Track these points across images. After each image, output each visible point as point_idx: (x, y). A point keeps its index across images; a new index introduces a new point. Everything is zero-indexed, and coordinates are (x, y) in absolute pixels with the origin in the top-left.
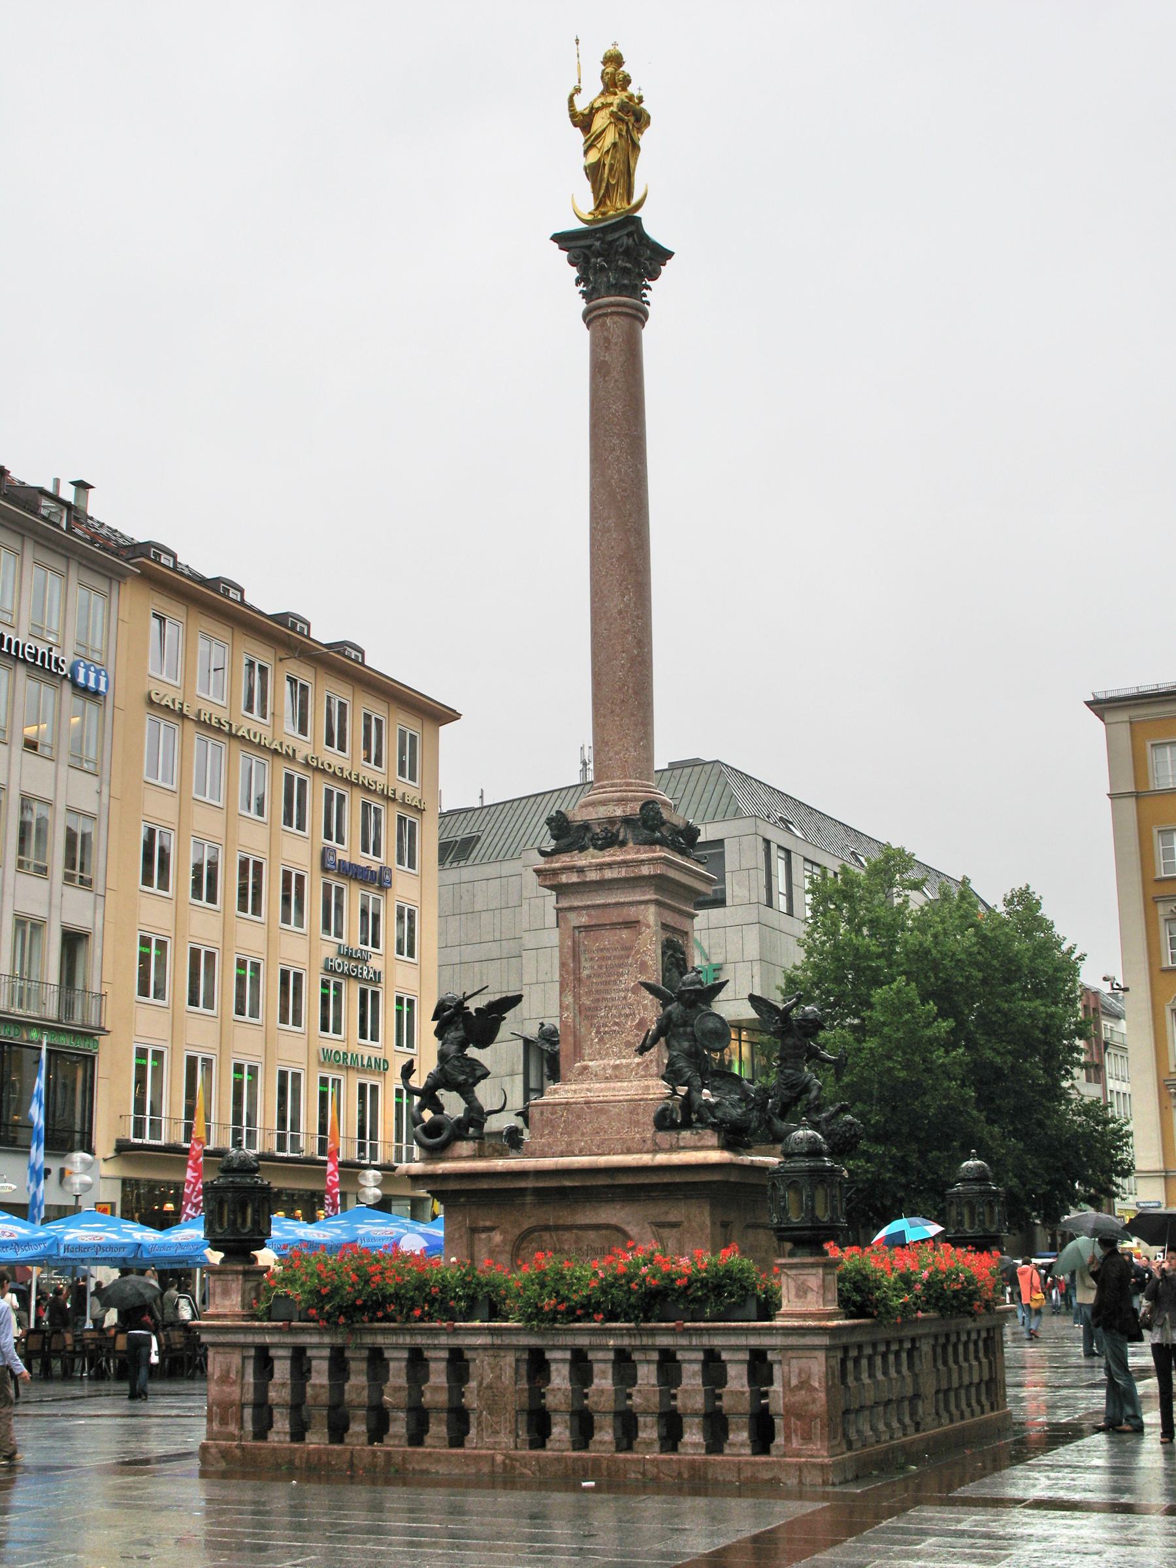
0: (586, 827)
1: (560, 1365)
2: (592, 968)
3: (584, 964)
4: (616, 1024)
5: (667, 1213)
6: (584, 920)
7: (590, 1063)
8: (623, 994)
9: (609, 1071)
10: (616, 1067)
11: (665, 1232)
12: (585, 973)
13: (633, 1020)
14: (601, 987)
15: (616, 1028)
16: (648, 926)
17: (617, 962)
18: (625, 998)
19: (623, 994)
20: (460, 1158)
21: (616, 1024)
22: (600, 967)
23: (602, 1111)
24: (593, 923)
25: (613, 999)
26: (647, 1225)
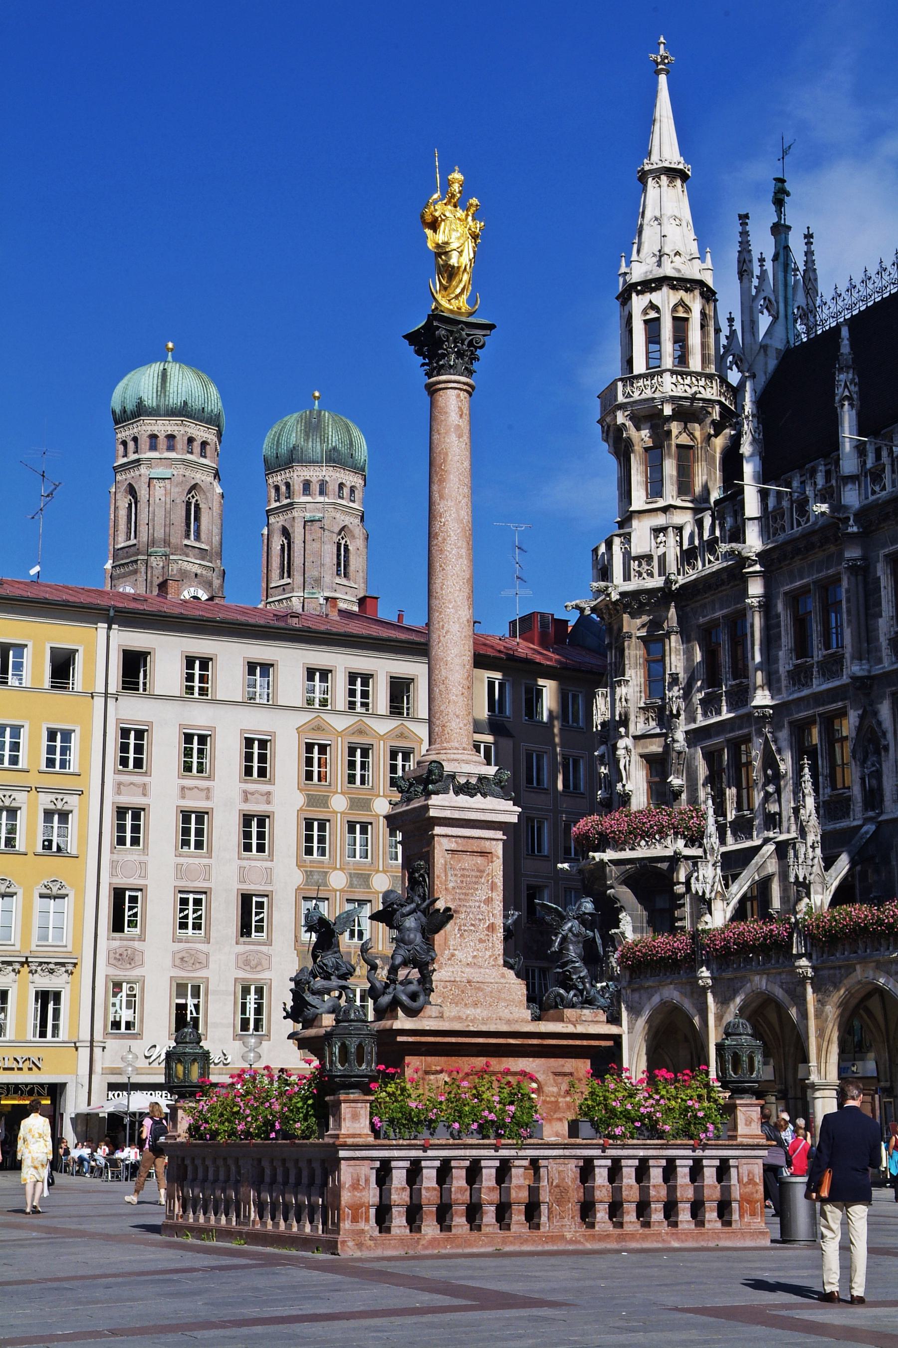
0: (453, 777)
1: (602, 1170)
2: (456, 882)
3: (450, 878)
4: (472, 925)
5: (563, 1066)
6: (453, 846)
7: (456, 952)
8: (477, 904)
9: (470, 959)
10: (474, 957)
11: (559, 1079)
12: (451, 885)
13: (484, 923)
14: (462, 897)
15: (472, 928)
16: (498, 858)
17: (474, 879)
18: (479, 907)
19: (477, 904)
20: (430, 1017)
21: (472, 925)
22: (462, 882)
23: (479, 989)
24: (459, 849)
25: (471, 907)
26: (550, 1074)
